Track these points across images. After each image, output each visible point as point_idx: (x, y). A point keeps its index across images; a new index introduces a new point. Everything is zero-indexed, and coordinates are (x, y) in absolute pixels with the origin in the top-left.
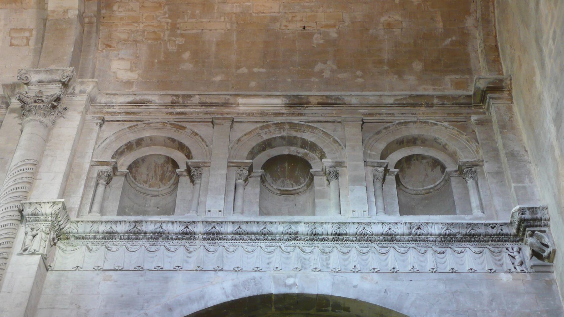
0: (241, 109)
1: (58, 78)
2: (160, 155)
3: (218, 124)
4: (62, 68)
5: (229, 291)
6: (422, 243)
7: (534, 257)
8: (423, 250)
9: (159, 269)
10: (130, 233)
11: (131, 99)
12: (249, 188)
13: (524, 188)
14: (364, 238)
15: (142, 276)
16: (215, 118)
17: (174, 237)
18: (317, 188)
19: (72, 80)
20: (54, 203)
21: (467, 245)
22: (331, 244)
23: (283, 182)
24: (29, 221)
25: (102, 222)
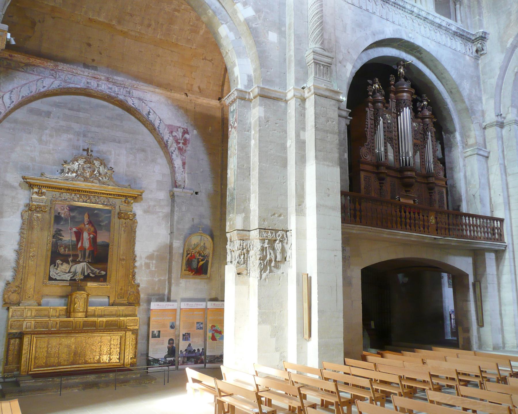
22: (421, 21)
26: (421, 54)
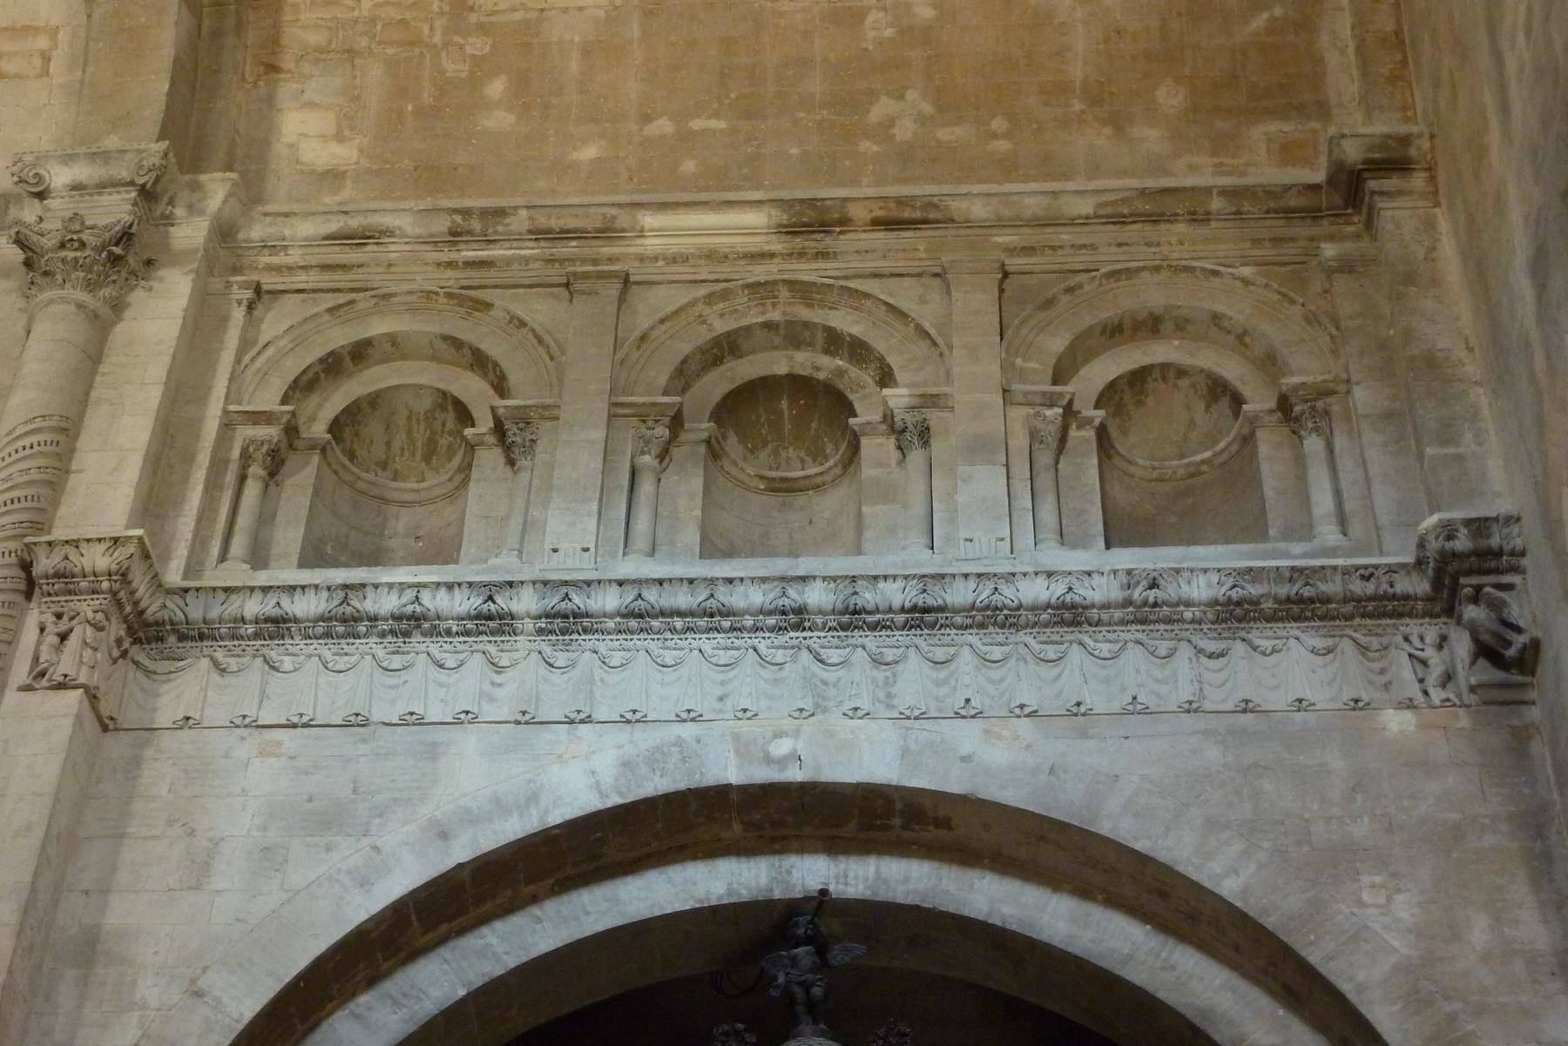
0: (651, 244)
1: (125, 175)
2: (421, 387)
3: (584, 293)
4: (136, 146)
5: (607, 777)
6: (1162, 627)
7: (1482, 662)
8: (1163, 647)
9: (412, 720)
10: (330, 619)
11: (334, 225)
12: (671, 478)
13: (1459, 458)
14: (994, 618)
15: (364, 741)
16: (575, 274)
17: (454, 629)
18: (868, 471)
19: (164, 179)
20: (116, 540)
21: (1293, 629)
22: (900, 637)
23: (776, 453)
24: (49, 595)
25: (252, 589)
26: (945, 823)
